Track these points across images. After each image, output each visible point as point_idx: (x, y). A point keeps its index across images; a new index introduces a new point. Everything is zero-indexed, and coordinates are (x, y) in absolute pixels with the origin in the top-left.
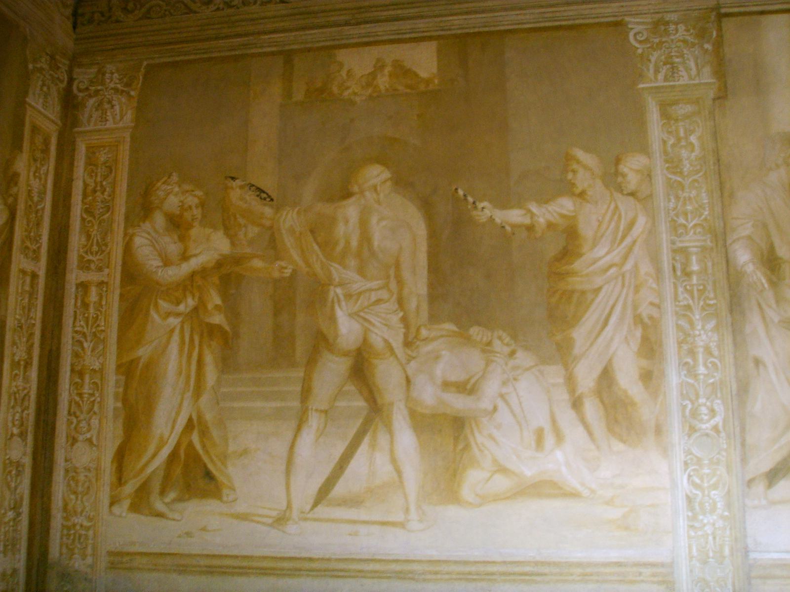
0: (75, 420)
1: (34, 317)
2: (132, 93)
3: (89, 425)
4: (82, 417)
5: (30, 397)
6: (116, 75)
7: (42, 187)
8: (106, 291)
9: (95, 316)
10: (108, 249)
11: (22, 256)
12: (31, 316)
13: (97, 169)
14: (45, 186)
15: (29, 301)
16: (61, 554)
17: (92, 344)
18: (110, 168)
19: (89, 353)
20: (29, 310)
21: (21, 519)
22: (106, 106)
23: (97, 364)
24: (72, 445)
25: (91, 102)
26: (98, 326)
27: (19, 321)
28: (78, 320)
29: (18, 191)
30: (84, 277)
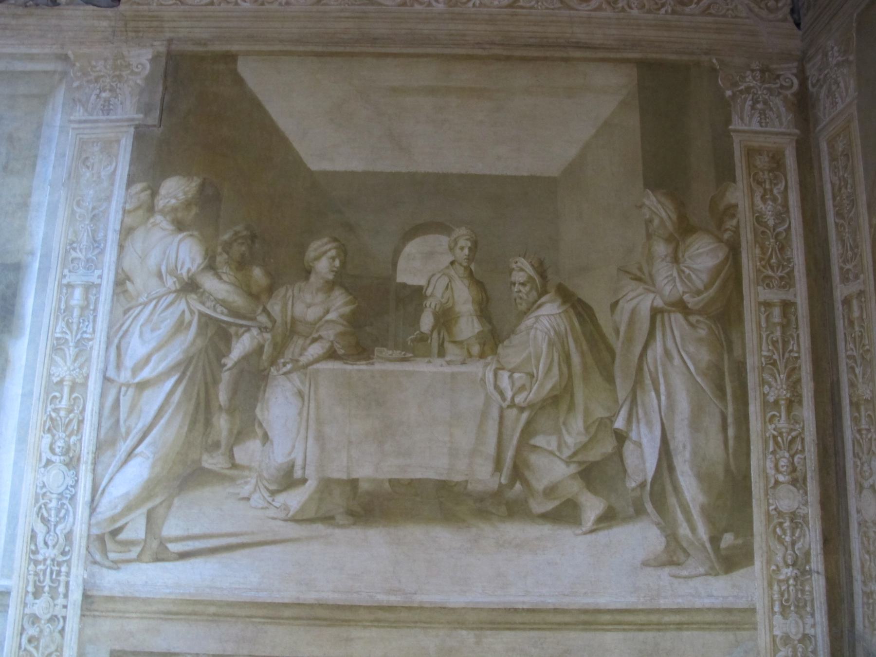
0: (859, 463)
1: (795, 349)
2: (851, 58)
3: (871, 469)
4: (864, 459)
5: (803, 440)
6: (836, 48)
7: (780, 207)
8: (865, 301)
9: (860, 334)
10: (860, 250)
11: (760, 288)
12: (791, 348)
13: (838, 163)
14: (786, 205)
15: (783, 333)
16: (864, 626)
17: (862, 368)
18: (847, 155)
19: (861, 380)
20: (785, 343)
21: (811, 579)
22: (834, 87)
23: (868, 392)
24: (861, 492)
25: (824, 91)
26: (864, 345)
27: (770, 358)
28: (848, 343)
29: (738, 222)
30: (846, 292)
